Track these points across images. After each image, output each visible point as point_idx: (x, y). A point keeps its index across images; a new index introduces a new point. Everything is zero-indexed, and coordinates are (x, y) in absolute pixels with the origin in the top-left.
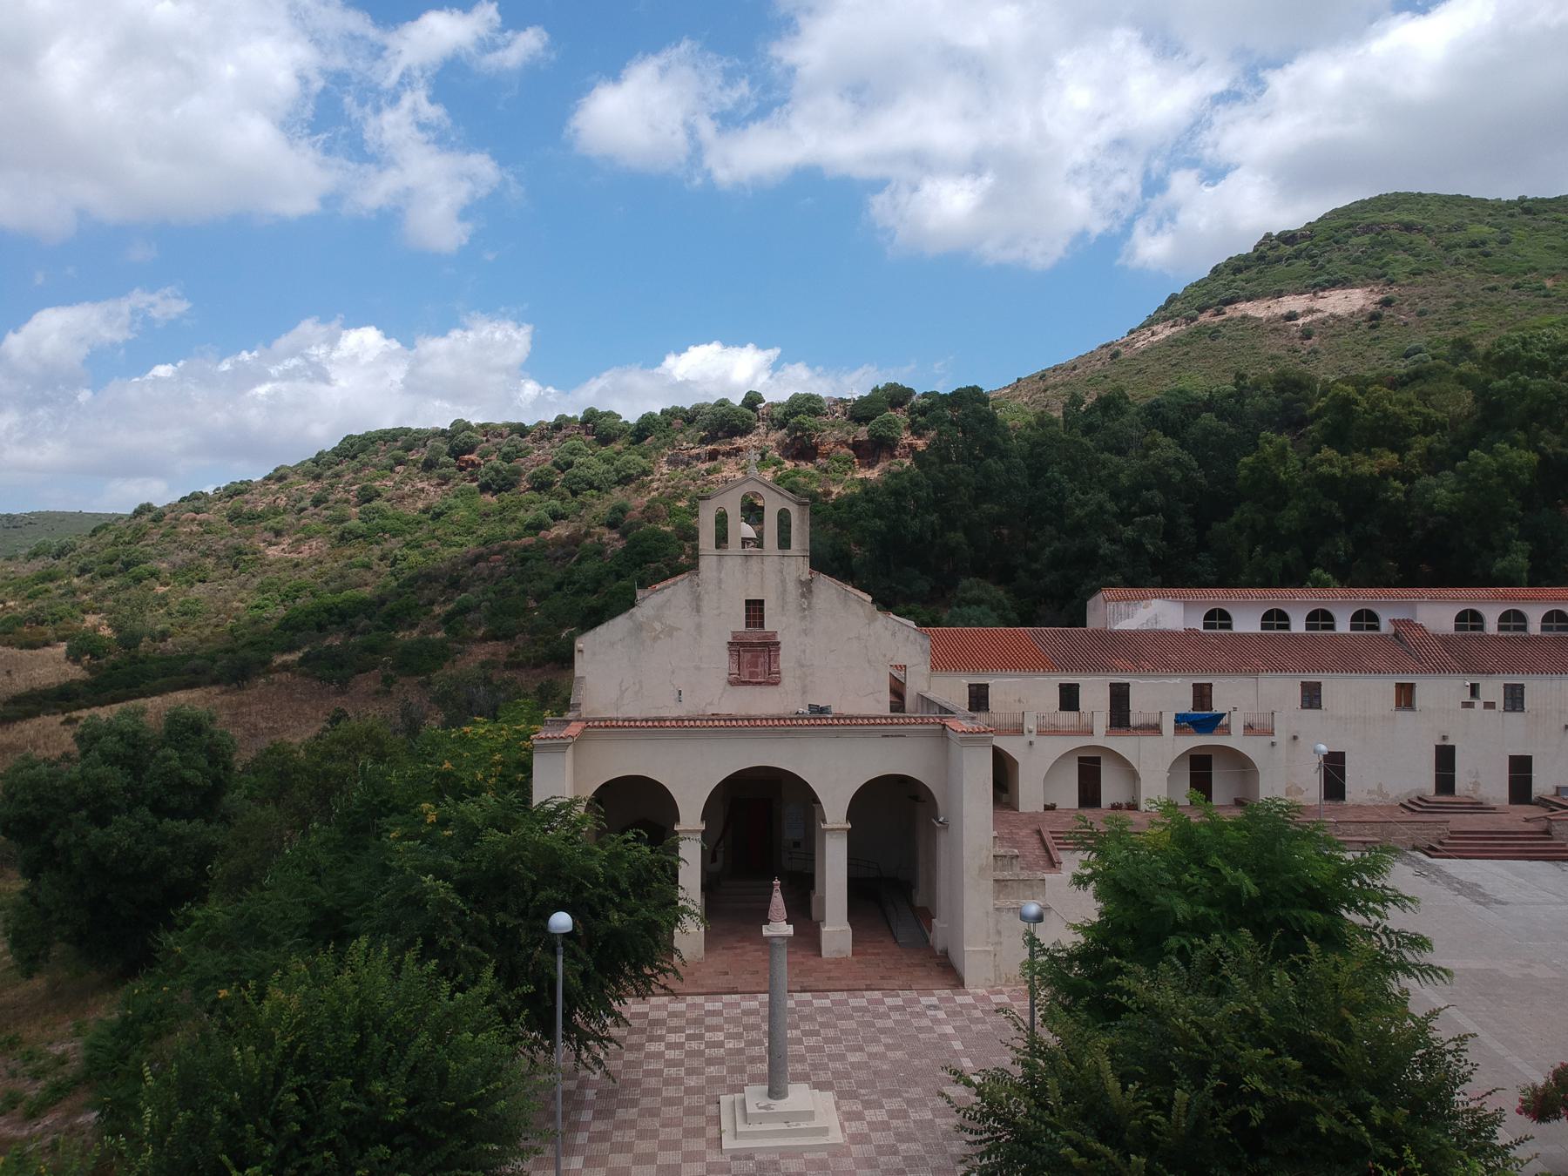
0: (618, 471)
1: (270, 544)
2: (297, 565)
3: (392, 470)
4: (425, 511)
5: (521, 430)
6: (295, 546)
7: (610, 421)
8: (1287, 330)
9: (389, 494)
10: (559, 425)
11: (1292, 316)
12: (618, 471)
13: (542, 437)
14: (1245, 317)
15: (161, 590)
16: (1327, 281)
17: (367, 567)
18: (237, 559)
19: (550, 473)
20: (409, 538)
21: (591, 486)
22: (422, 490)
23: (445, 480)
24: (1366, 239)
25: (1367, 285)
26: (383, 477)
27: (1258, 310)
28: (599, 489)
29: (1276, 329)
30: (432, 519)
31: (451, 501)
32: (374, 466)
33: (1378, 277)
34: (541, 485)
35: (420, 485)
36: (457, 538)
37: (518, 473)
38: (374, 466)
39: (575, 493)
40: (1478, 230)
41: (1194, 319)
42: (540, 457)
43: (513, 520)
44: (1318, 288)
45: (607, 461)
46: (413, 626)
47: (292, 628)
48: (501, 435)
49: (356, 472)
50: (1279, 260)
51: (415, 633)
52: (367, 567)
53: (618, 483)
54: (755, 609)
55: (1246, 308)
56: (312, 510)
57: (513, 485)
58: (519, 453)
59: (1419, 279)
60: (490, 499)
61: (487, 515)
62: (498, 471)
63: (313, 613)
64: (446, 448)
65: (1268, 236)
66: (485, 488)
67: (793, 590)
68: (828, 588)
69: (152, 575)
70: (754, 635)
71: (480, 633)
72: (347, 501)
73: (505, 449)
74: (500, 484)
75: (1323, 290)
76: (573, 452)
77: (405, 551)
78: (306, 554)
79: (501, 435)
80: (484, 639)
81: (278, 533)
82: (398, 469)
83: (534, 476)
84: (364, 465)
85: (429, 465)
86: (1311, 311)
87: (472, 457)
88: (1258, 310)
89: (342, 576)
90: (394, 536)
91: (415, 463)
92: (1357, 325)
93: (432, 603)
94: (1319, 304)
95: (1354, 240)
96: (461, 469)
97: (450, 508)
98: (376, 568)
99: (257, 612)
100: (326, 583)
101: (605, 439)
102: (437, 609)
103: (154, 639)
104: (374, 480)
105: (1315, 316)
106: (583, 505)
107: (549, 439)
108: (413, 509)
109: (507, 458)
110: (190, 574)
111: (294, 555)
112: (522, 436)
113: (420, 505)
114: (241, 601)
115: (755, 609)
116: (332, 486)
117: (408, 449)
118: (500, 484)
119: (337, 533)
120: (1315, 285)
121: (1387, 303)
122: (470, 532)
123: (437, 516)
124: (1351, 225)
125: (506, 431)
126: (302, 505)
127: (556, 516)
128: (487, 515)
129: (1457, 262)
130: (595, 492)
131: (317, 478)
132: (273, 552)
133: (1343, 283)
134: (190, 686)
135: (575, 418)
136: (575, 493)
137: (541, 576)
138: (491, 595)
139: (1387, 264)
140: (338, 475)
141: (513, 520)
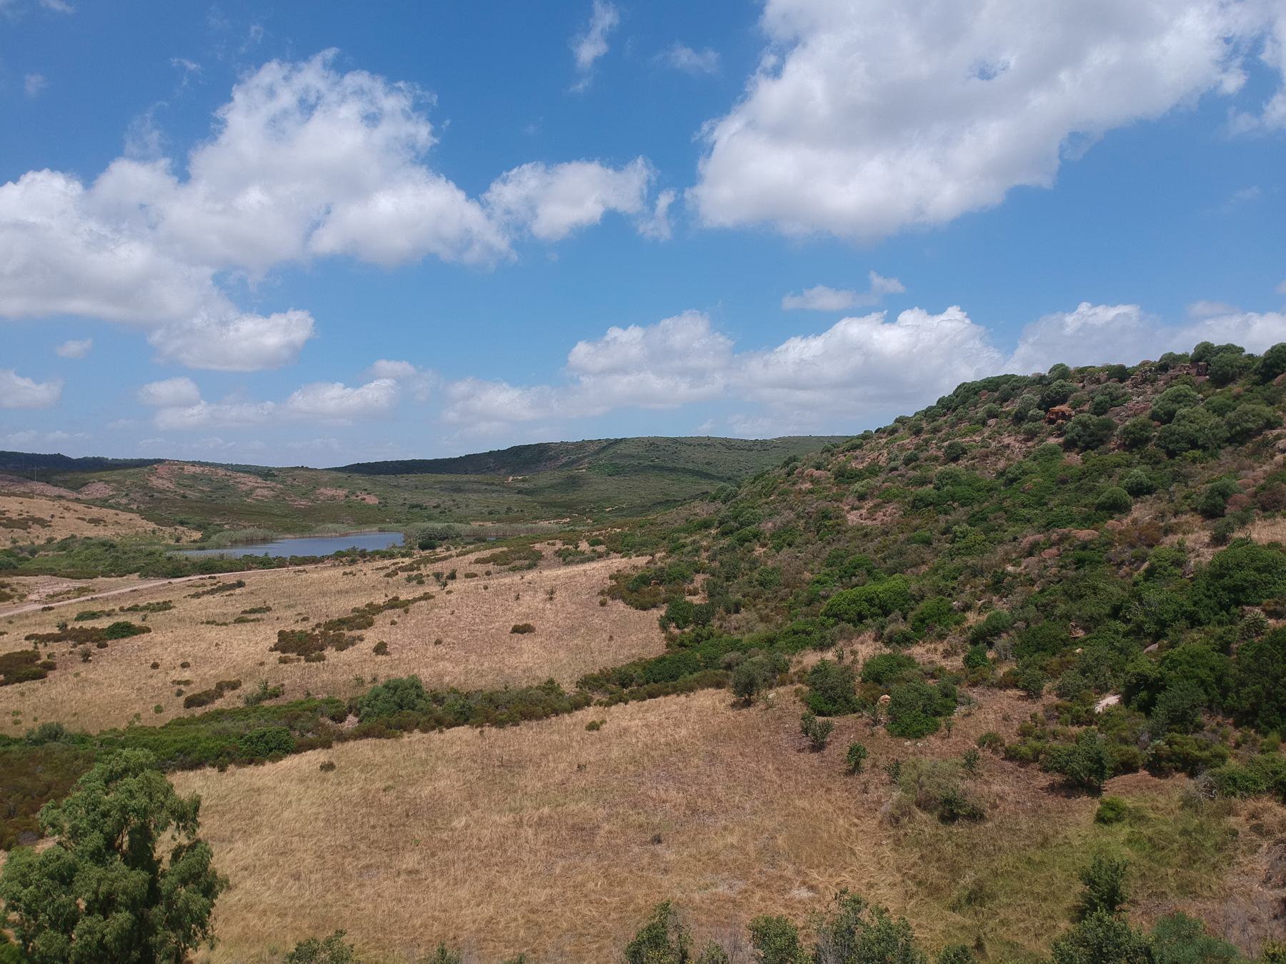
0: (1231, 425)
1: (853, 509)
2: (866, 535)
3: (984, 424)
4: (1001, 474)
5: (1120, 374)
6: (871, 515)
7: (1228, 356)
9: (975, 452)
10: (1166, 364)
12: (1231, 425)
13: (1144, 381)
15: (759, 551)
17: (927, 542)
18: (825, 523)
19: (1144, 427)
20: (976, 508)
21: (1194, 445)
22: (1008, 446)
23: (1031, 435)
26: (974, 432)
28: (1204, 448)
30: (1005, 485)
31: (1029, 464)
32: (970, 419)
34: (1134, 442)
35: (1006, 441)
36: (1026, 511)
37: (1110, 427)
38: (970, 419)
39: (1171, 454)
42: (1140, 404)
43: (1091, 490)
45: (1220, 411)
46: (941, 637)
47: (835, 616)
48: (1098, 381)
49: (953, 426)
51: (941, 648)
52: (927, 542)
53: (1230, 441)
56: (902, 469)
57: (1102, 442)
58: (1115, 400)
60: (1074, 459)
61: (1064, 482)
62: (1085, 426)
63: (854, 602)
64: (1037, 399)
66: (1069, 446)
69: (755, 536)
71: (1002, 670)
72: (936, 459)
73: (1098, 398)
74: (1088, 440)
76: (1177, 399)
77: (965, 526)
78: (878, 523)
79: (1098, 381)
80: (1004, 685)
81: (862, 497)
82: (992, 422)
83: (1126, 431)
84: (960, 420)
85: (1019, 418)
87: (1064, 408)
89: (901, 553)
90: (963, 505)
91: (1008, 414)
93: (967, 608)
96: (1051, 422)
97: (1025, 473)
98: (935, 545)
99: (818, 587)
100: (884, 559)
101: (1222, 380)
102: (972, 618)
103: (728, 611)
104: (964, 435)
106: (1176, 477)
107: (1153, 382)
108: (987, 475)
109: (1100, 409)
110: (783, 539)
111: (869, 522)
112: (1121, 381)
113: (1001, 465)
114: (812, 571)
116: (927, 442)
117: (1004, 399)
118: (1088, 440)
119: (910, 498)
122: (1041, 503)
123: (1011, 481)
125: (1103, 376)
126: (893, 464)
127: (1138, 491)
128: (1064, 482)
130: (1198, 453)
131: (918, 432)
132: (853, 518)
134: (719, 685)
135: (1185, 356)
136: (1171, 454)
137: (1095, 590)
138: (1031, 611)
140: (936, 430)
141: (1091, 490)
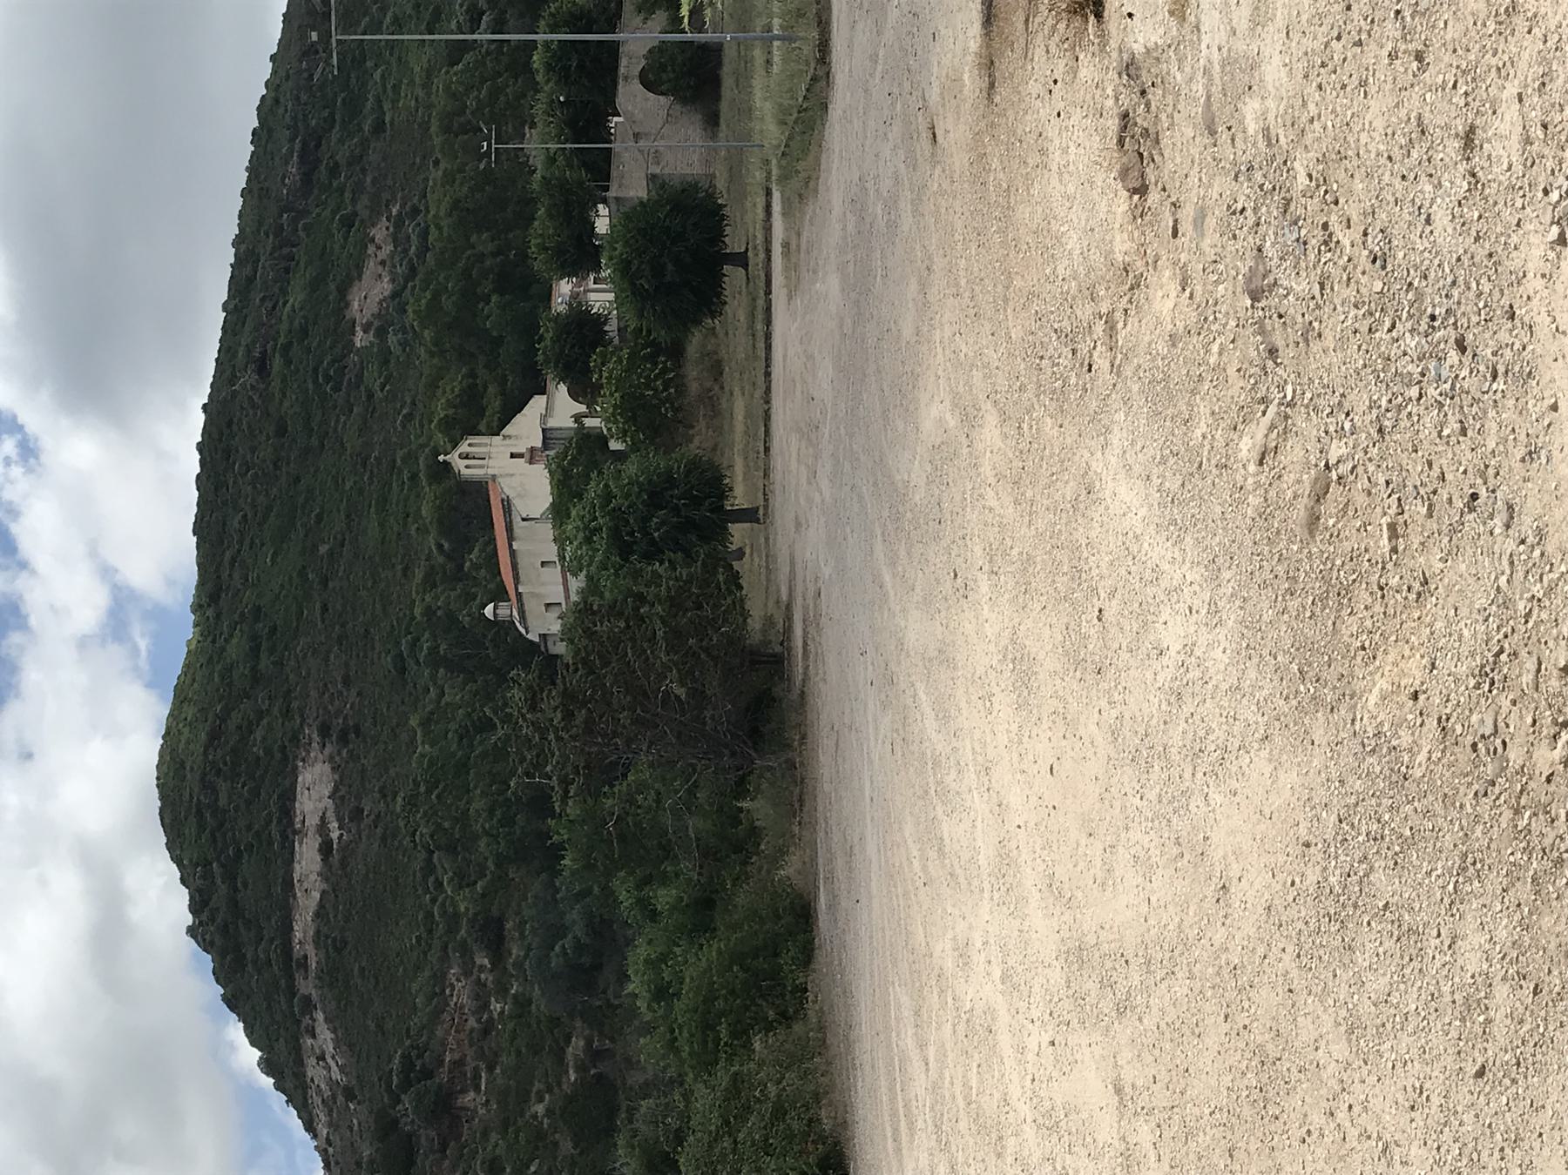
8: (344, 848)
11: (326, 849)
14: (317, 915)
16: (279, 821)
24: (223, 786)
25: (295, 768)
27: (307, 902)
29: (344, 863)
33: (285, 758)
40: (236, 648)
41: (307, 1000)
44: (289, 832)
50: (234, 904)
54: (513, 456)
55: (303, 926)
59: (295, 704)
65: (191, 931)
67: (507, 442)
68: (507, 430)
70: (527, 456)
75: (291, 823)
86: (323, 827)
88: (307, 902)
92: (350, 752)
94: (313, 821)
95: (222, 802)
105: (330, 815)
115: (513, 456)
120: (284, 837)
121: (325, 731)
124: (199, 813)
129: (280, 664)
133: (289, 796)
139: (269, 752)
